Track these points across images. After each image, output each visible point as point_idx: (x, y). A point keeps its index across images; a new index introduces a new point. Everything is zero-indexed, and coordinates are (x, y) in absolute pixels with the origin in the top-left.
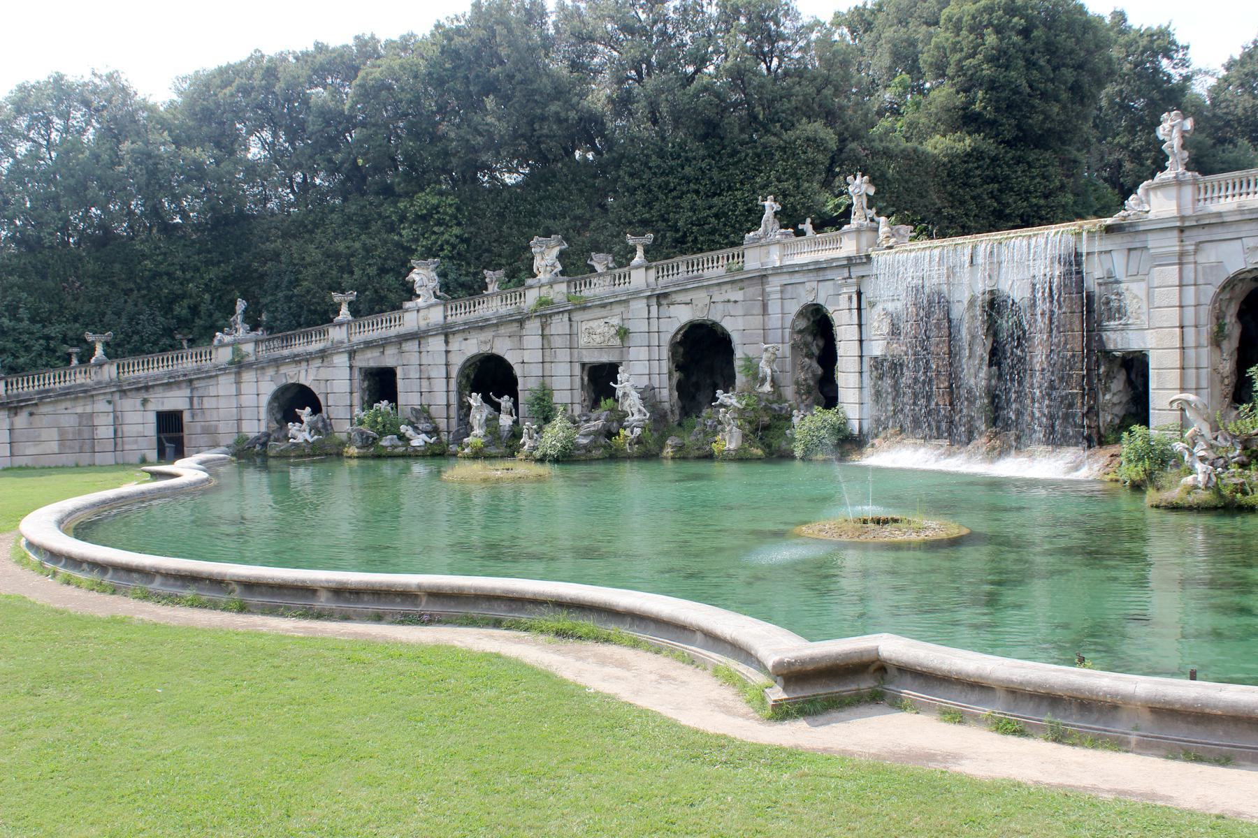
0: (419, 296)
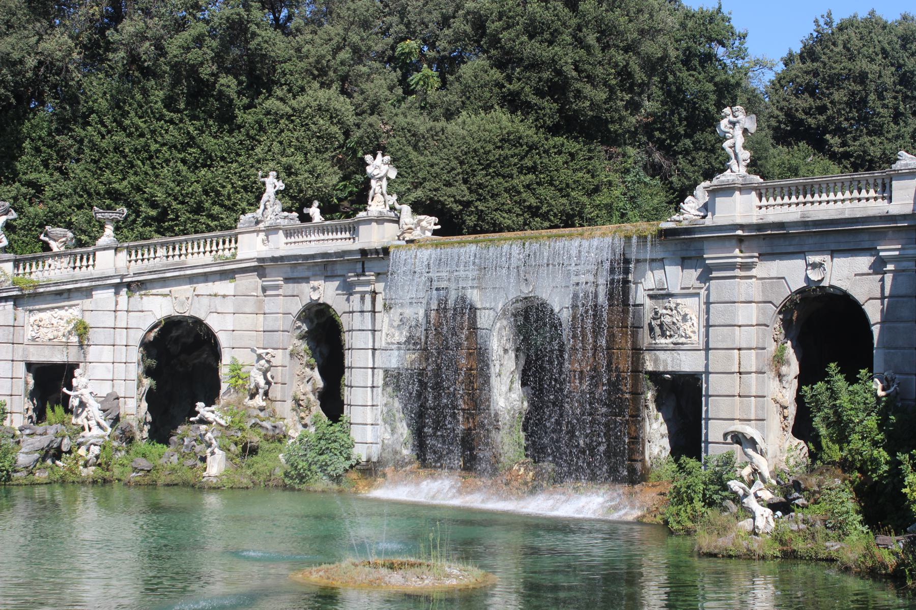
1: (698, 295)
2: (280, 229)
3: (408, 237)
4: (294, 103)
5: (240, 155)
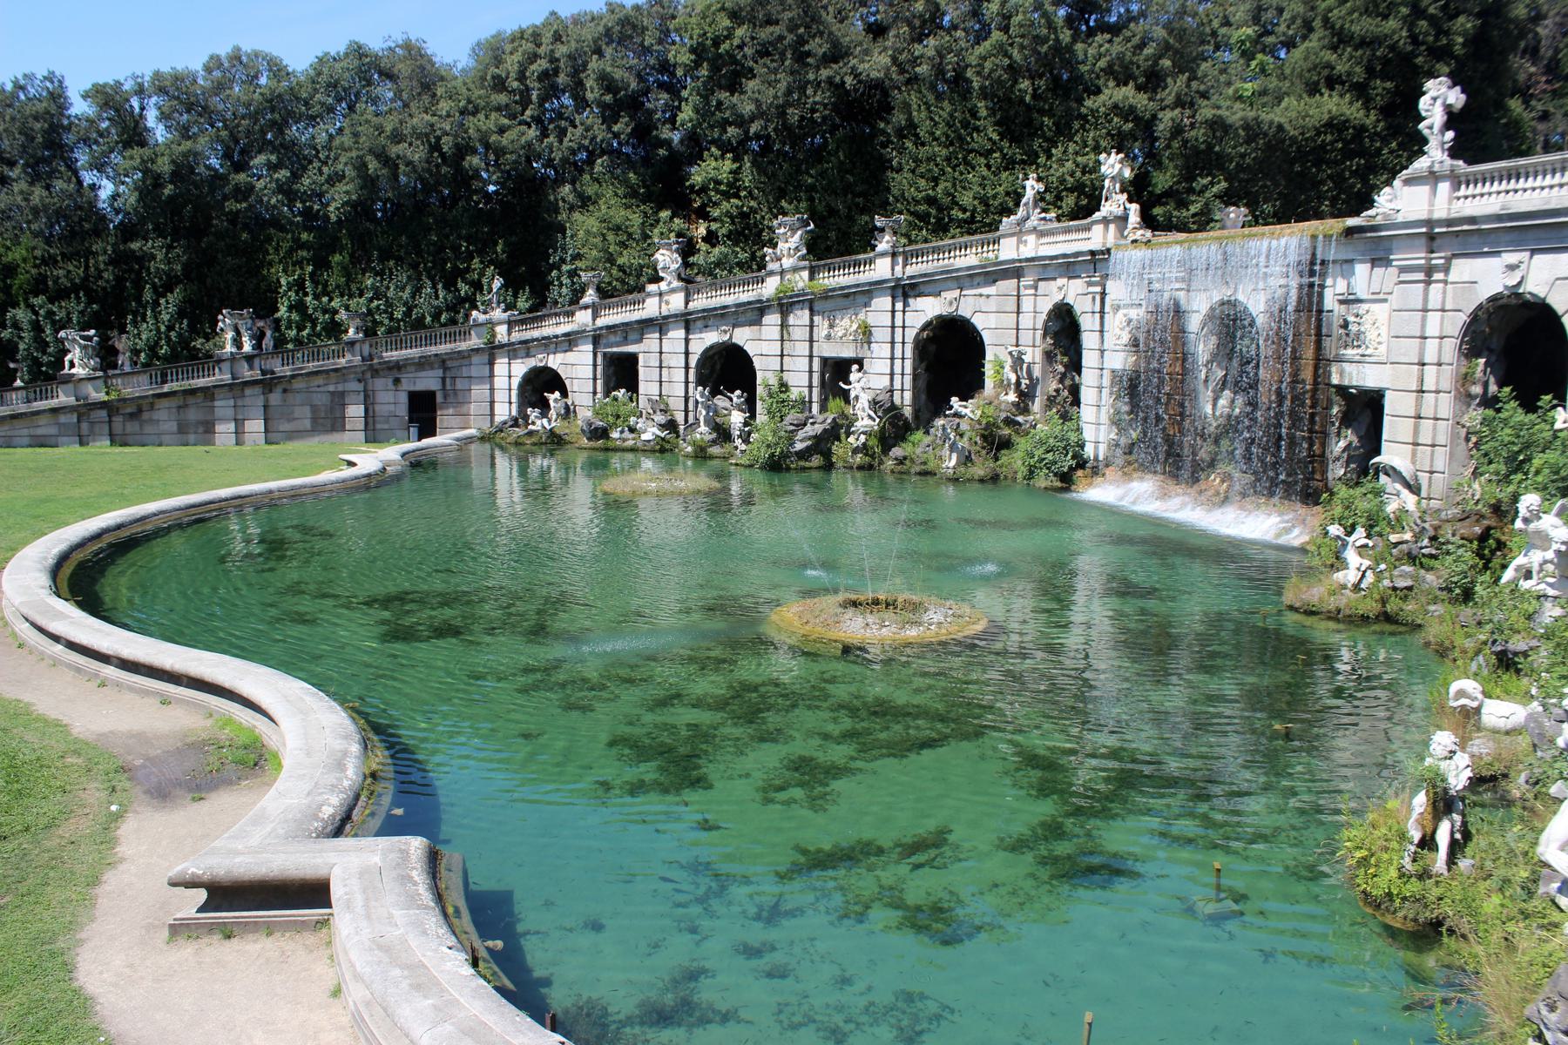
0: (662, 279)
1: (1385, 300)
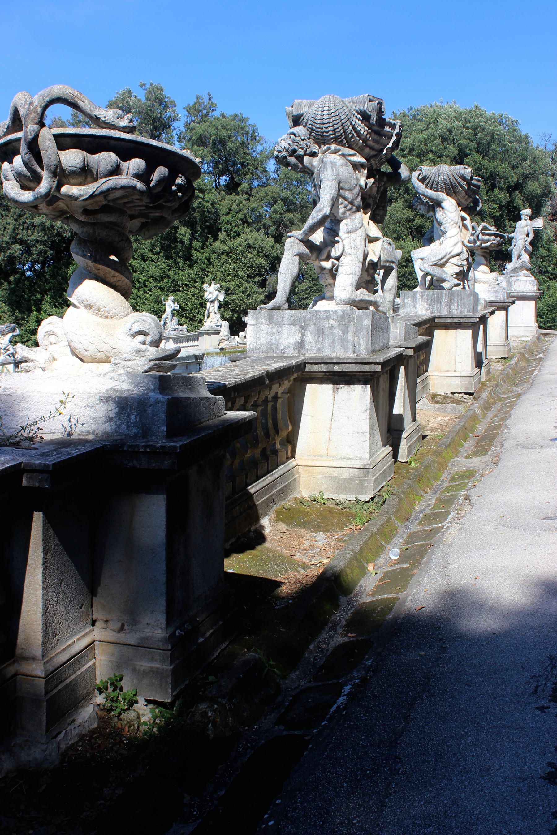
2: (170, 338)
3: (222, 346)
4: (230, 244)
5: (197, 282)
